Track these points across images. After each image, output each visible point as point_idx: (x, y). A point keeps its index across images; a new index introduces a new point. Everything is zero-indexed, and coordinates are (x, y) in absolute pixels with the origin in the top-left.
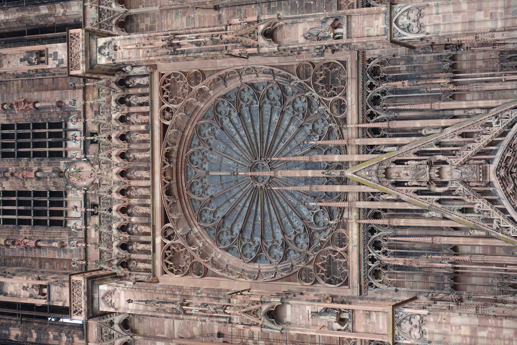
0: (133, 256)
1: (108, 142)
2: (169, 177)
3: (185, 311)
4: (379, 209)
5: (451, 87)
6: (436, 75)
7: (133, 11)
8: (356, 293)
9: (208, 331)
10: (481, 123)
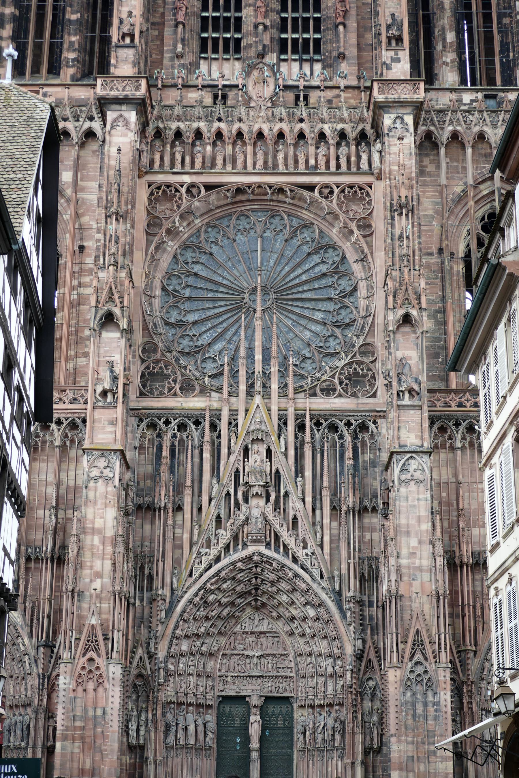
2: (256, 191)
3: (110, 216)
5: (344, 508)
6: (357, 492)
7: (443, 151)
8: (133, 405)
9: (85, 234)
10: (307, 537)
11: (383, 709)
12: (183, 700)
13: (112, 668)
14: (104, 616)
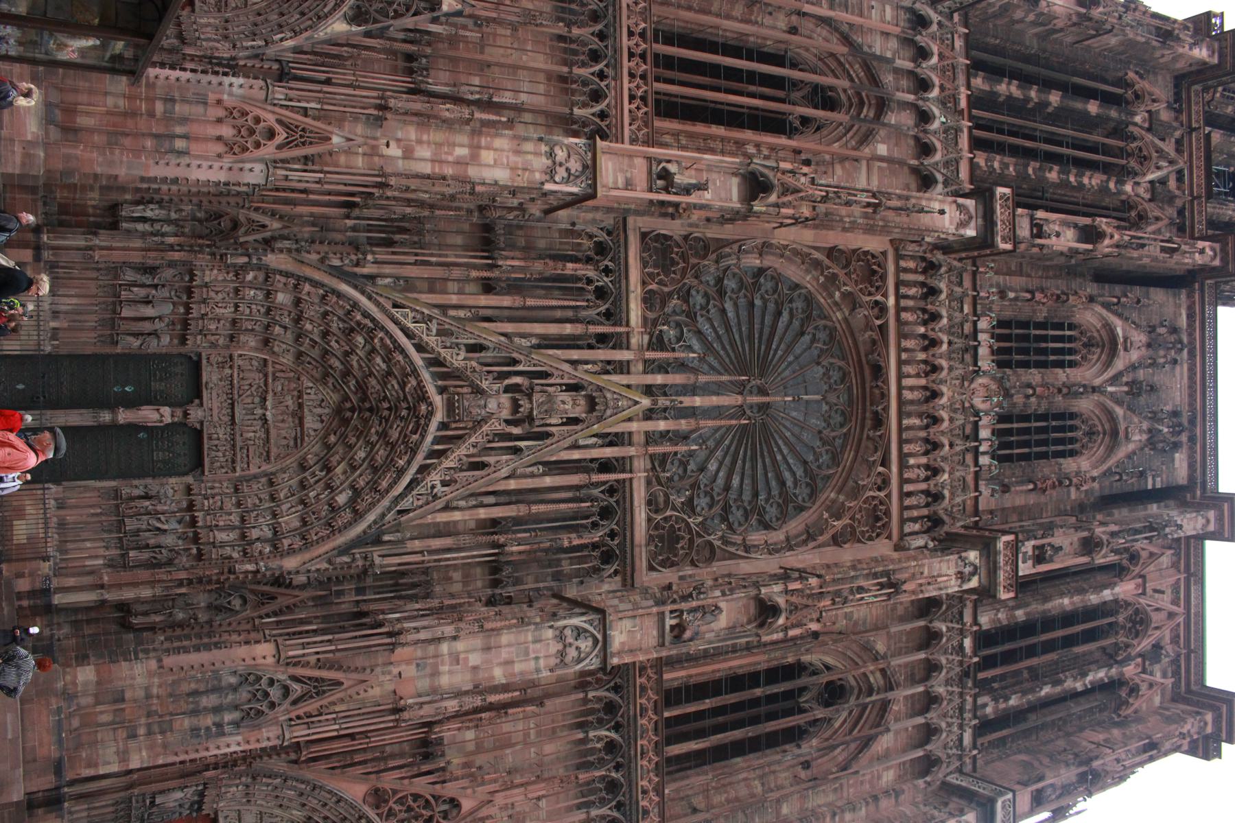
0: (921, 278)
2: (877, 391)
3: (874, 196)
5: (502, 539)
7: (922, 623)
10: (458, 486)
11: (197, 629)
12: (197, 296)
13: (259, 167)
14: (342, 159)
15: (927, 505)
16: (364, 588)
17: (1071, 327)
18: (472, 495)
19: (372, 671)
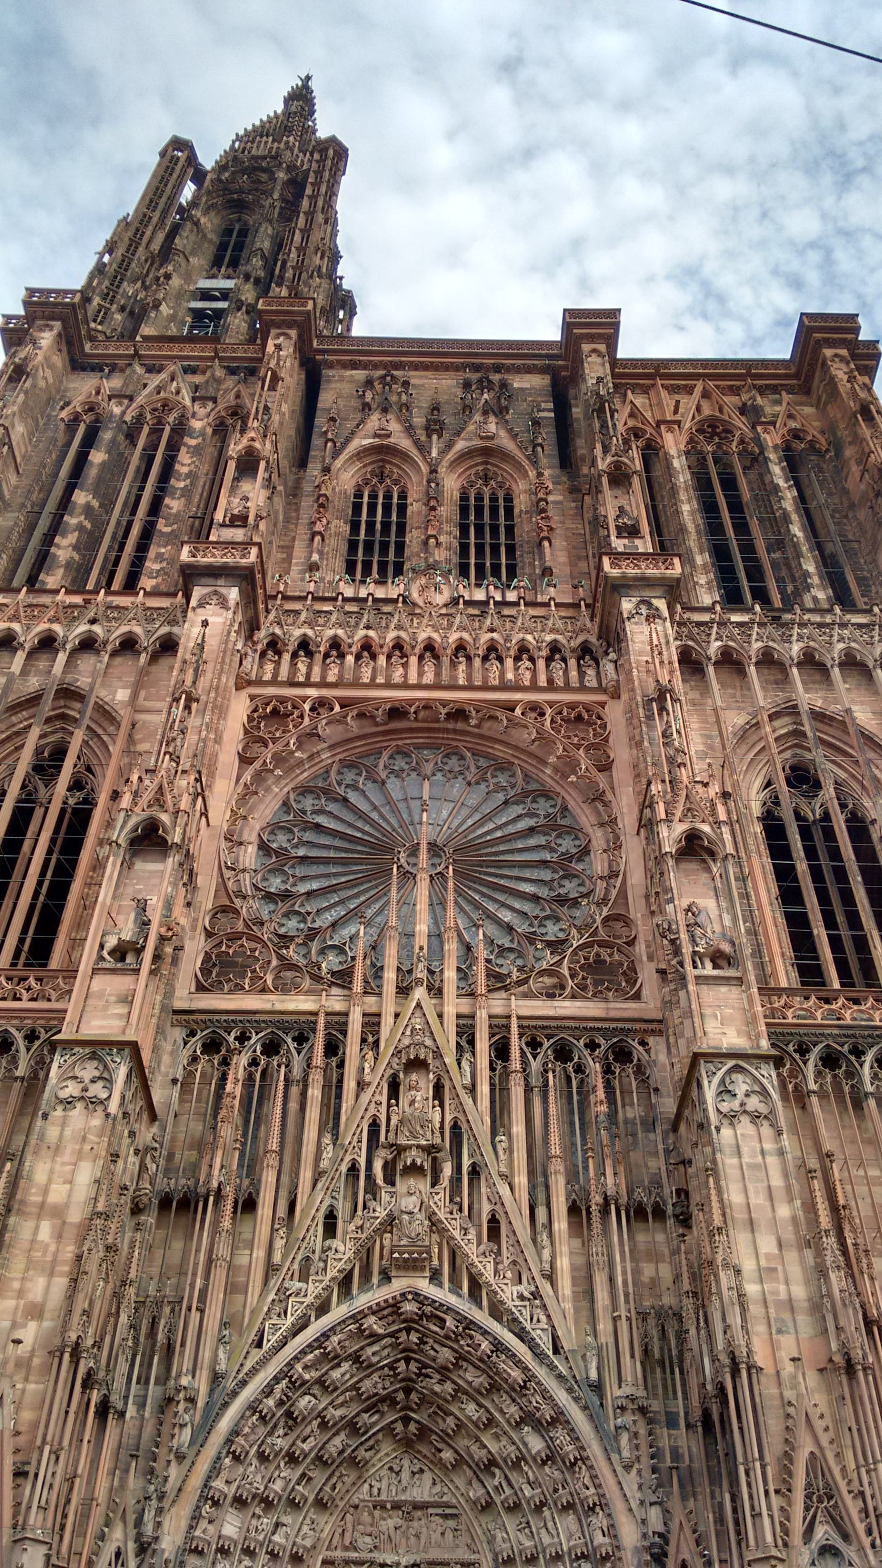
0: (287, 657)
1: (485, 628)
2: (422, 714)
3: (177, 700)
4: (344, 1053)
5: (597, 1199)
7: (711, 670)
8: (179, 1004)
10: (520, 1261)
15: (564, 660)
16: (667, 1414)
17: (359, 495)
18: (534, 1241)
19: (790, 1404)
